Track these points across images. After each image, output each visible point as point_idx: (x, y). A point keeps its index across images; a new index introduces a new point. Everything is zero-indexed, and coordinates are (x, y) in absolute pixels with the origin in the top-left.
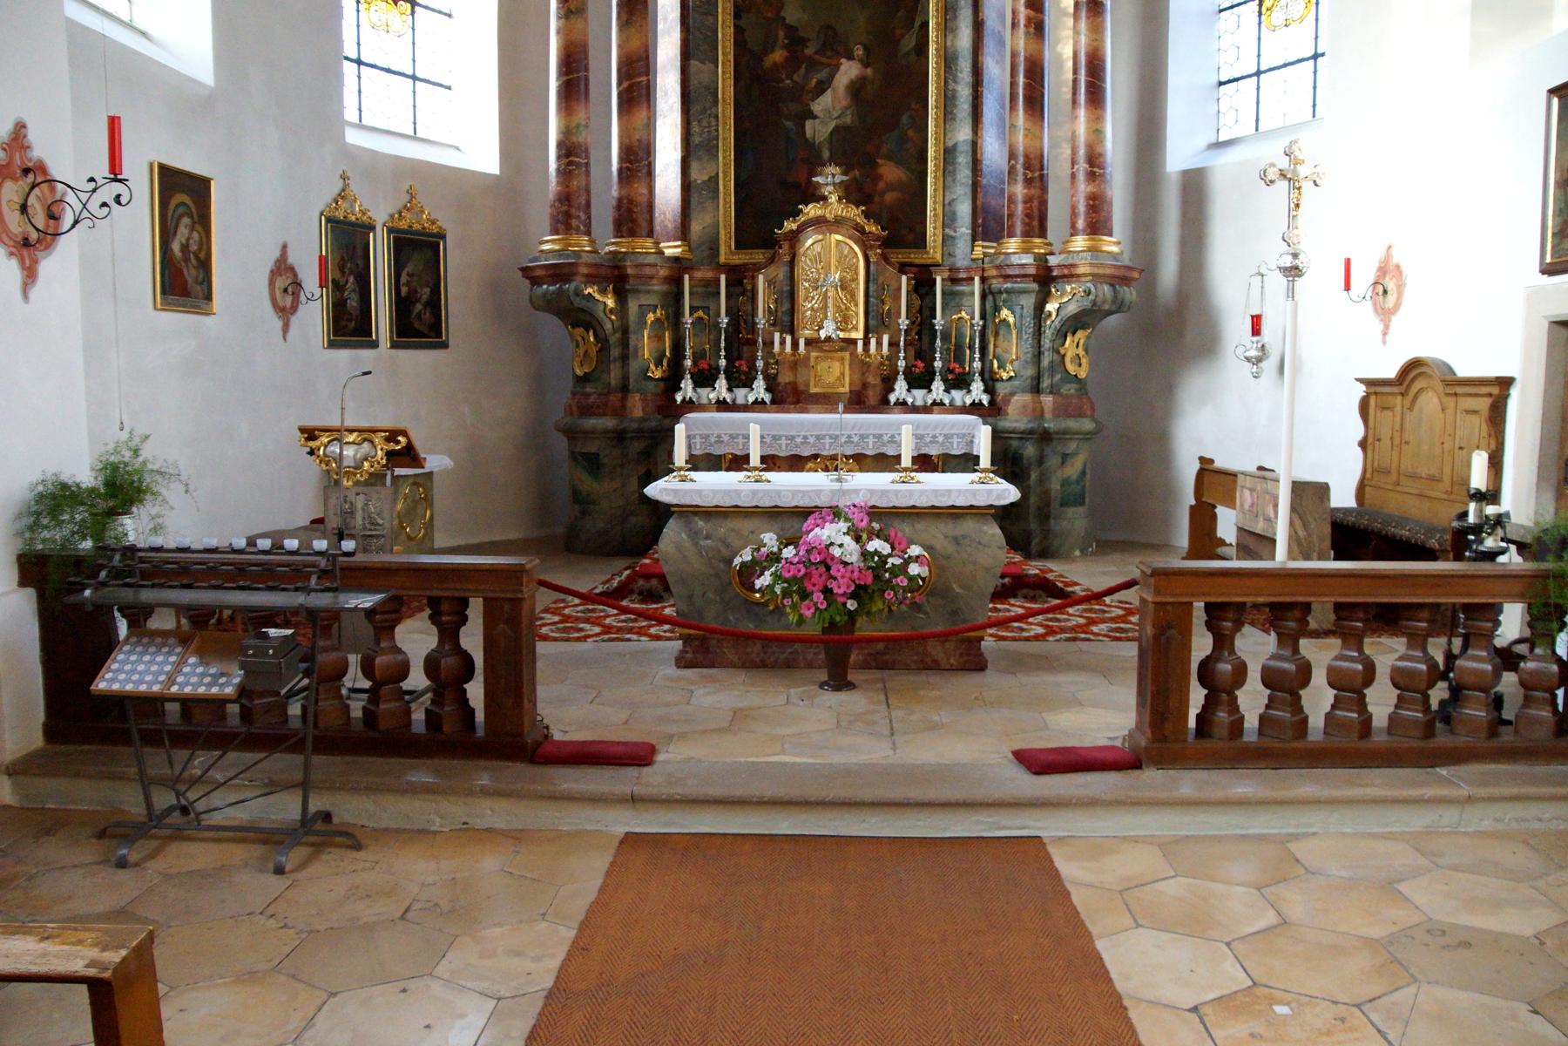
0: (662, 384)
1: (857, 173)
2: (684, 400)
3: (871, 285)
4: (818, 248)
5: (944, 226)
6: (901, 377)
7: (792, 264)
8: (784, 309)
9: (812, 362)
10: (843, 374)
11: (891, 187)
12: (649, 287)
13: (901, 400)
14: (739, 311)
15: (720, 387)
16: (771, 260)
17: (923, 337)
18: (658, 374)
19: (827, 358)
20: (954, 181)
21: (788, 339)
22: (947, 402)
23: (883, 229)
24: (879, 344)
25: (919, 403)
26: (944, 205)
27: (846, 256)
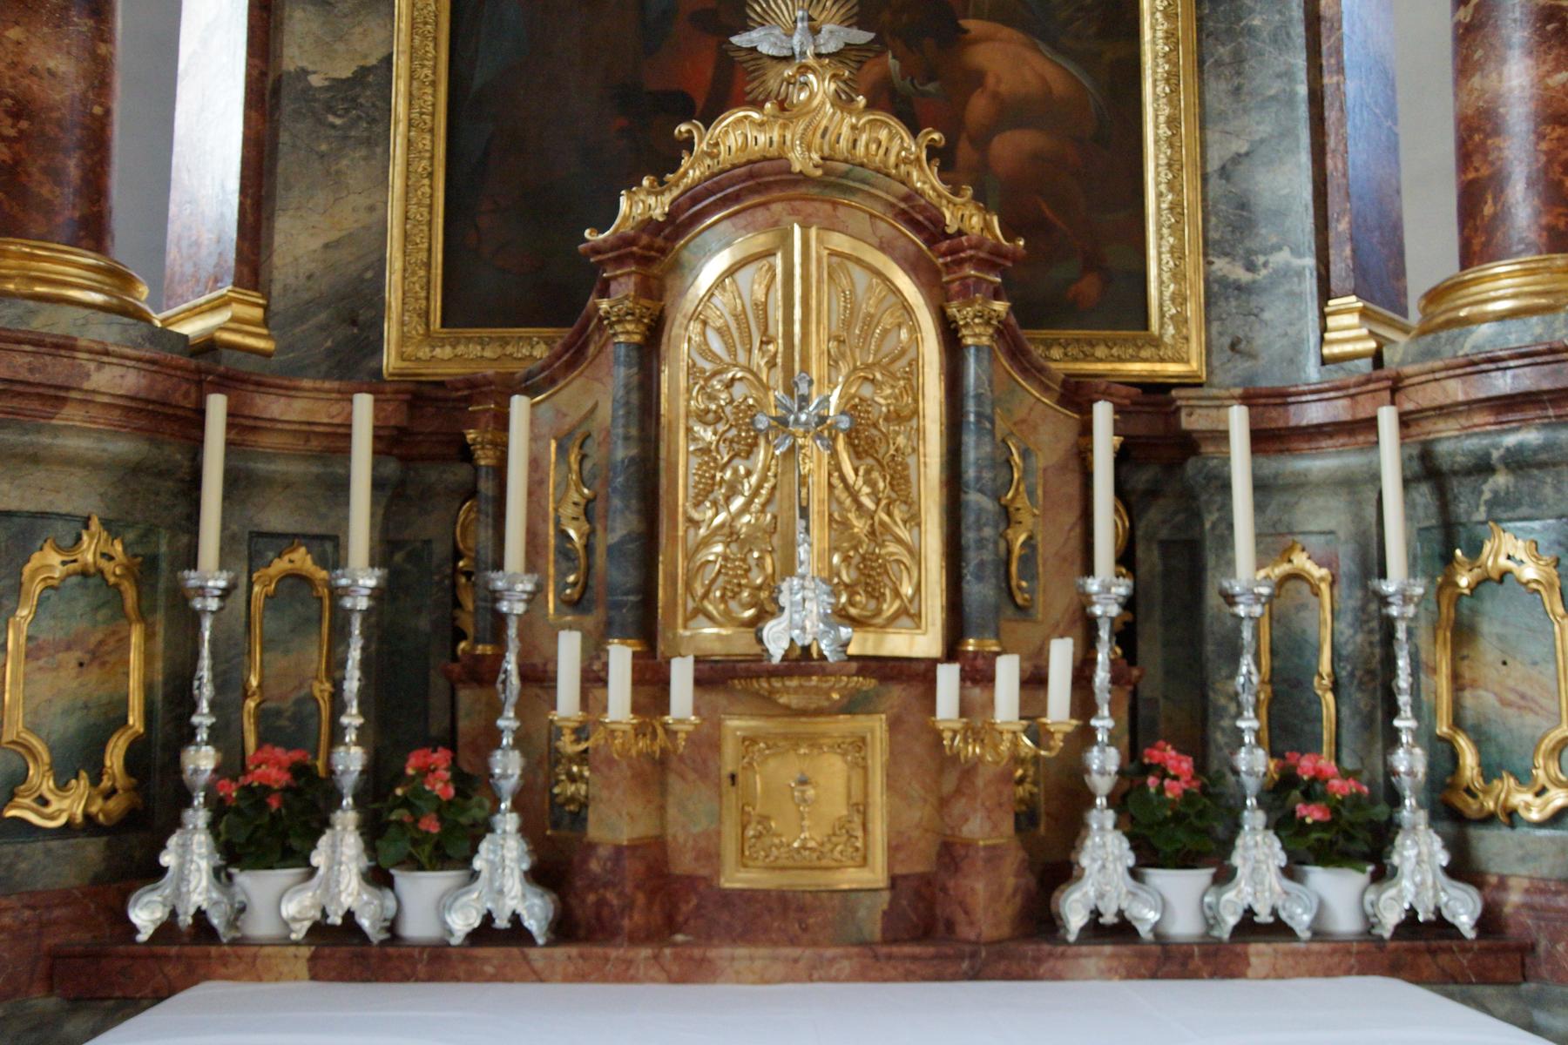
0: (93, 850)
1: (892, 63)
2: (167, 930)
3: (970, 440)
4: (752, 283)
5: (1209, 247)
6: (1101, 819)
7: (649, 350)
8: (613, 538)
9: (730, 759)
10: (861, 808)
11: (1012, 113)
12: (45, 440)
13: (1109, 918)
14: (457, 555)
15: (334, 861)
16: (574, 356)
17: (1142, 648)
18: (69, 805)
19: (795, 740)
20: (1237, 91)
21: (620, 658)
22: (1300, 919)
23: (1010, 230)
24: (1034, 681)
25: (1184, 926)
26: (1205, 179)
27: (870, 321)
